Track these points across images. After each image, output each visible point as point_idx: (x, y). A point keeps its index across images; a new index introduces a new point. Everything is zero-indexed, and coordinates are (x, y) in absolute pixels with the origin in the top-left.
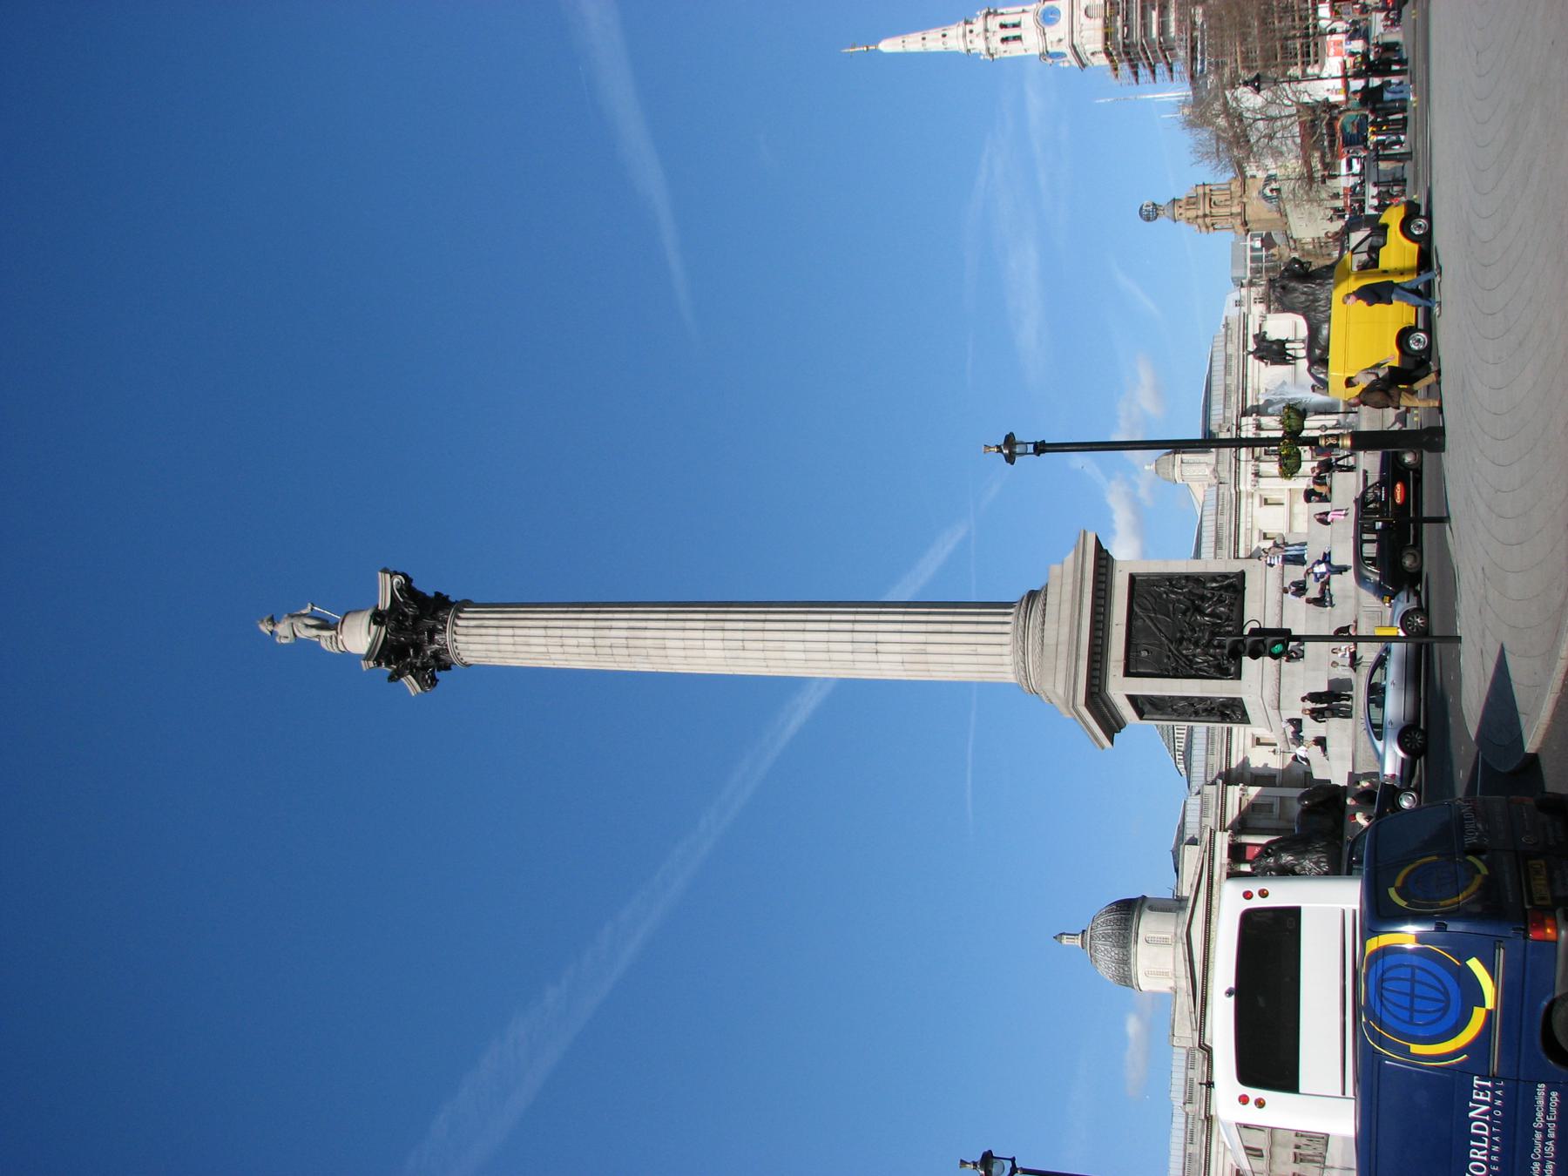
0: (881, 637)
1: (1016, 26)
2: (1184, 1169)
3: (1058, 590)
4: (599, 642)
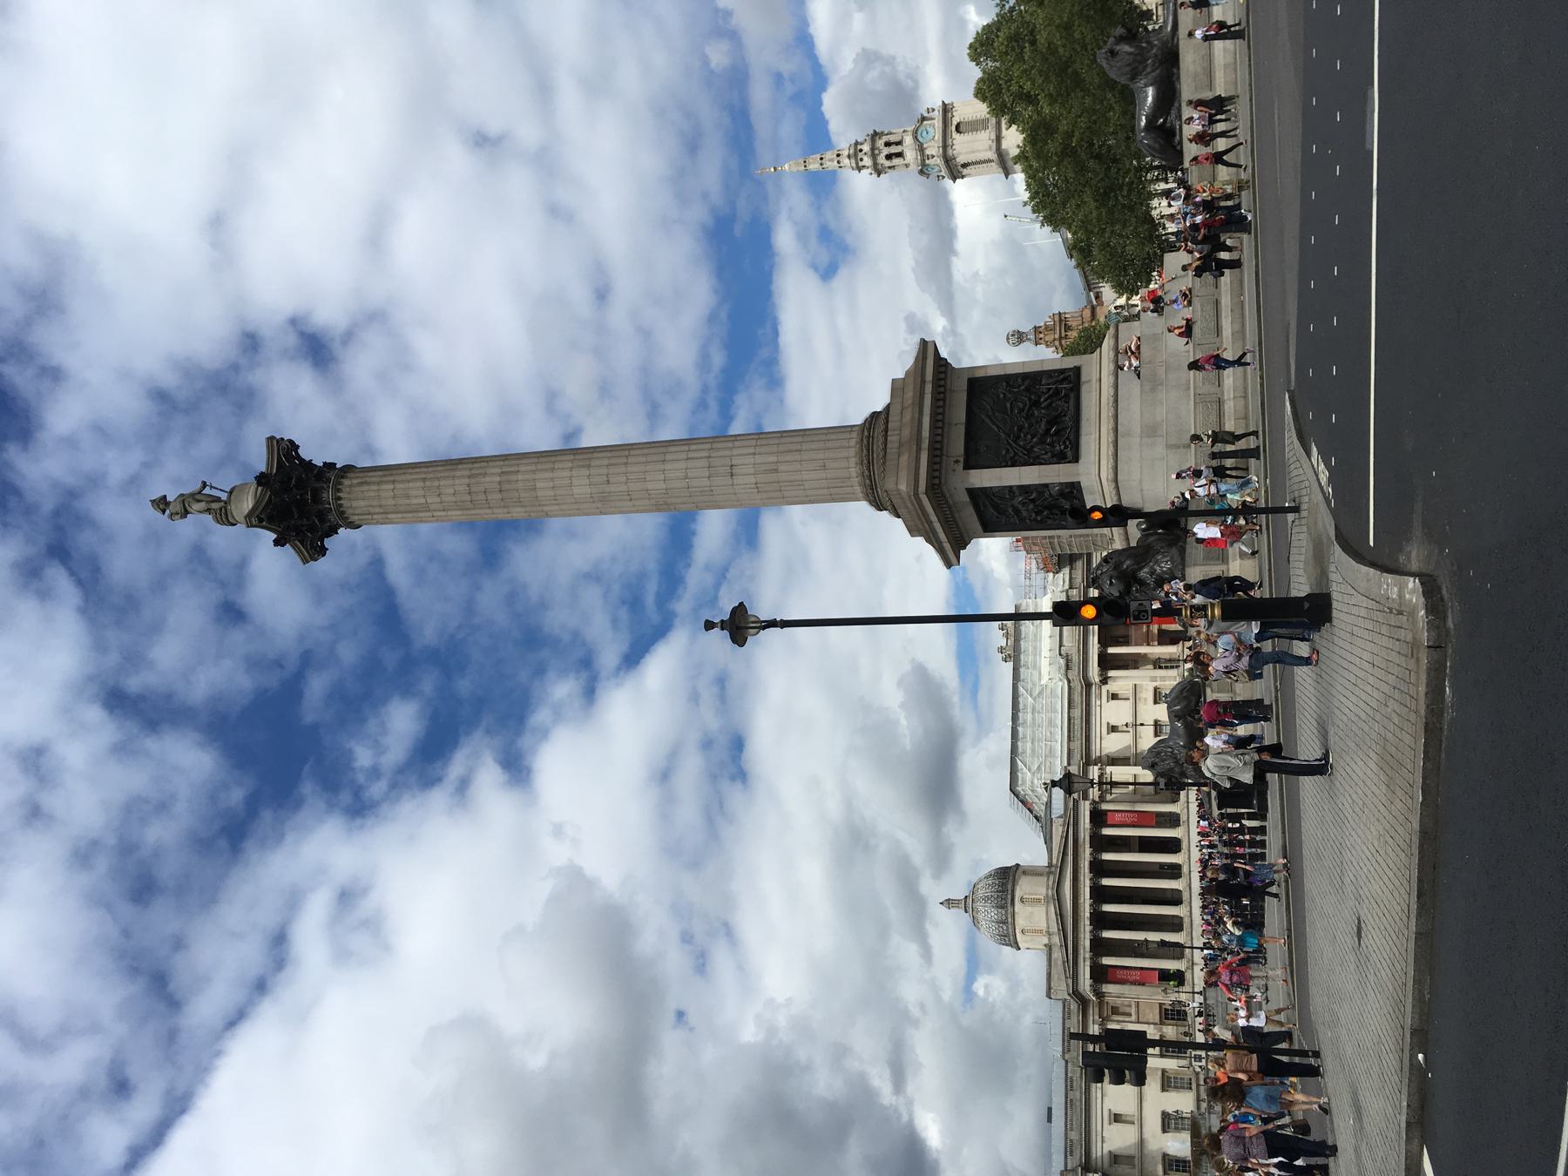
1: (899, 143)
2: (1066, 1114)
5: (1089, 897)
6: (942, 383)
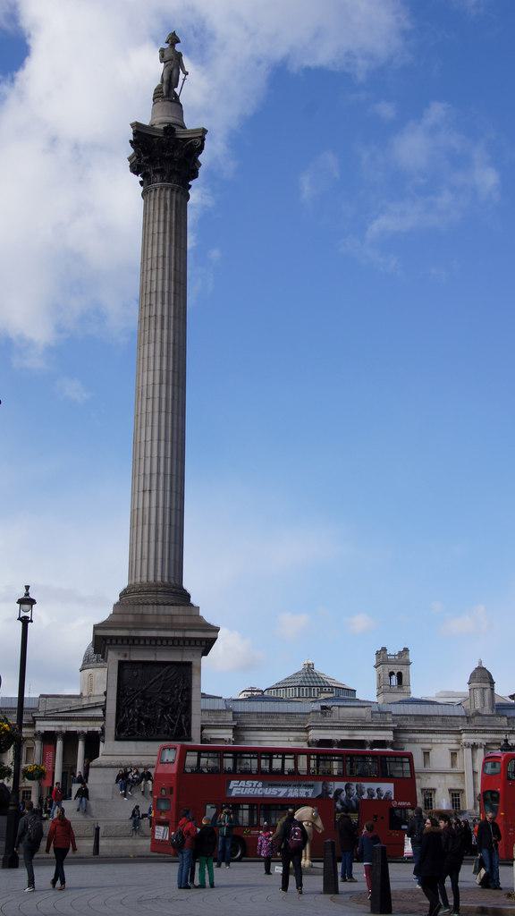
0: (154, 493)
3: (181, 613)
4: (154, 296)
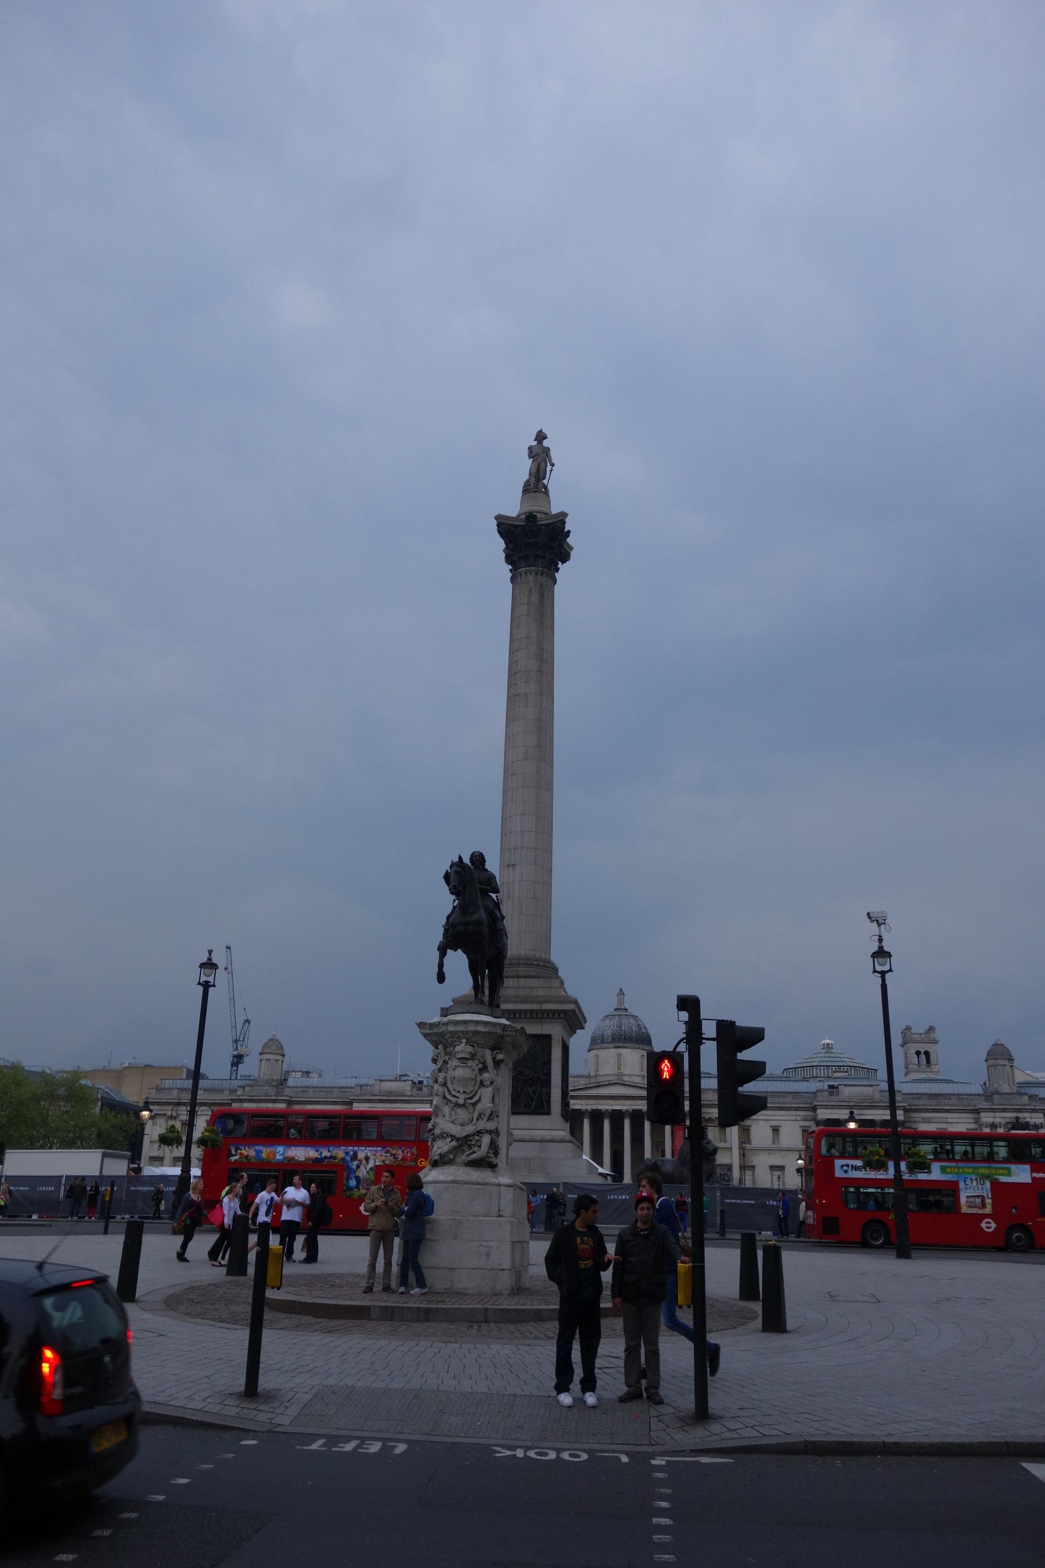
5: (614, 1108)
6: (556, 1016)
